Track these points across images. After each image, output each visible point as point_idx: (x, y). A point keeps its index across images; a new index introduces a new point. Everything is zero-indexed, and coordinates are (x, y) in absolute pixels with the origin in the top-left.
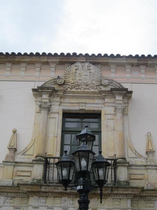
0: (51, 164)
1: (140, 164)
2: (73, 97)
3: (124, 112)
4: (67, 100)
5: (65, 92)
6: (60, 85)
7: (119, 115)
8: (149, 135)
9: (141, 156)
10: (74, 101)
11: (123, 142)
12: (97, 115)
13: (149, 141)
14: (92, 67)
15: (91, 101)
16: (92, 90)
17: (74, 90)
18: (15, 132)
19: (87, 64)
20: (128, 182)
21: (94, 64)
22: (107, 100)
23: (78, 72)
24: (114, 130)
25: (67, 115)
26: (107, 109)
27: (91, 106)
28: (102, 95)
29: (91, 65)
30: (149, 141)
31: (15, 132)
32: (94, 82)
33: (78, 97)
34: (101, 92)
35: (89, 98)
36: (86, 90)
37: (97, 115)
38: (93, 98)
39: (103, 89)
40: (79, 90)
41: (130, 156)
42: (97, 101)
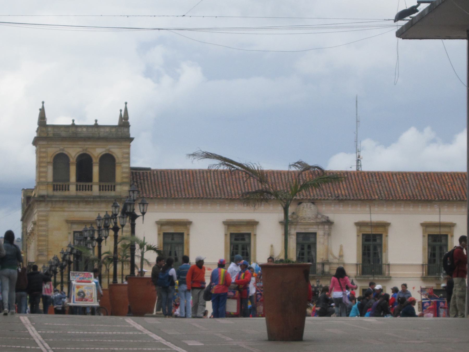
0: (286, 256)
1: (335, 262)
2: (301, 225)
3: (329, 235)
4: (298, 227)
5: (297, 222)
6: (294, 219)
7: (326, 237)
8: (341, 246)
9: (336, 258)
10: (302, 227)
11: (328, 251)
12: (315, 234)
13: (341, 250)
14: (312, 206)
15: (311, 227)
16: (312, 221)
17: (302, 221)
18: (272, 246)
19: (309, 204)
20: (329, 273)
21: (313, 203)
22: (320, 227)
23: (304, 209)
24: (323, 244)
25: (298, 234)
26: (320, 233)
27: (311, 230)
28: (318, 224)
29: (312, 204)
30: (341, 250)
31: (272, 246)
32: (313, 216)
33: (304, 225)
34: (317, 223)
35: (311, 225)
36: (309, 221)
37: (315, 234)
38: (312, 225)
39: (318, 221)
40: (305, 222)
41: (331, 259)
42: (314, 227)
